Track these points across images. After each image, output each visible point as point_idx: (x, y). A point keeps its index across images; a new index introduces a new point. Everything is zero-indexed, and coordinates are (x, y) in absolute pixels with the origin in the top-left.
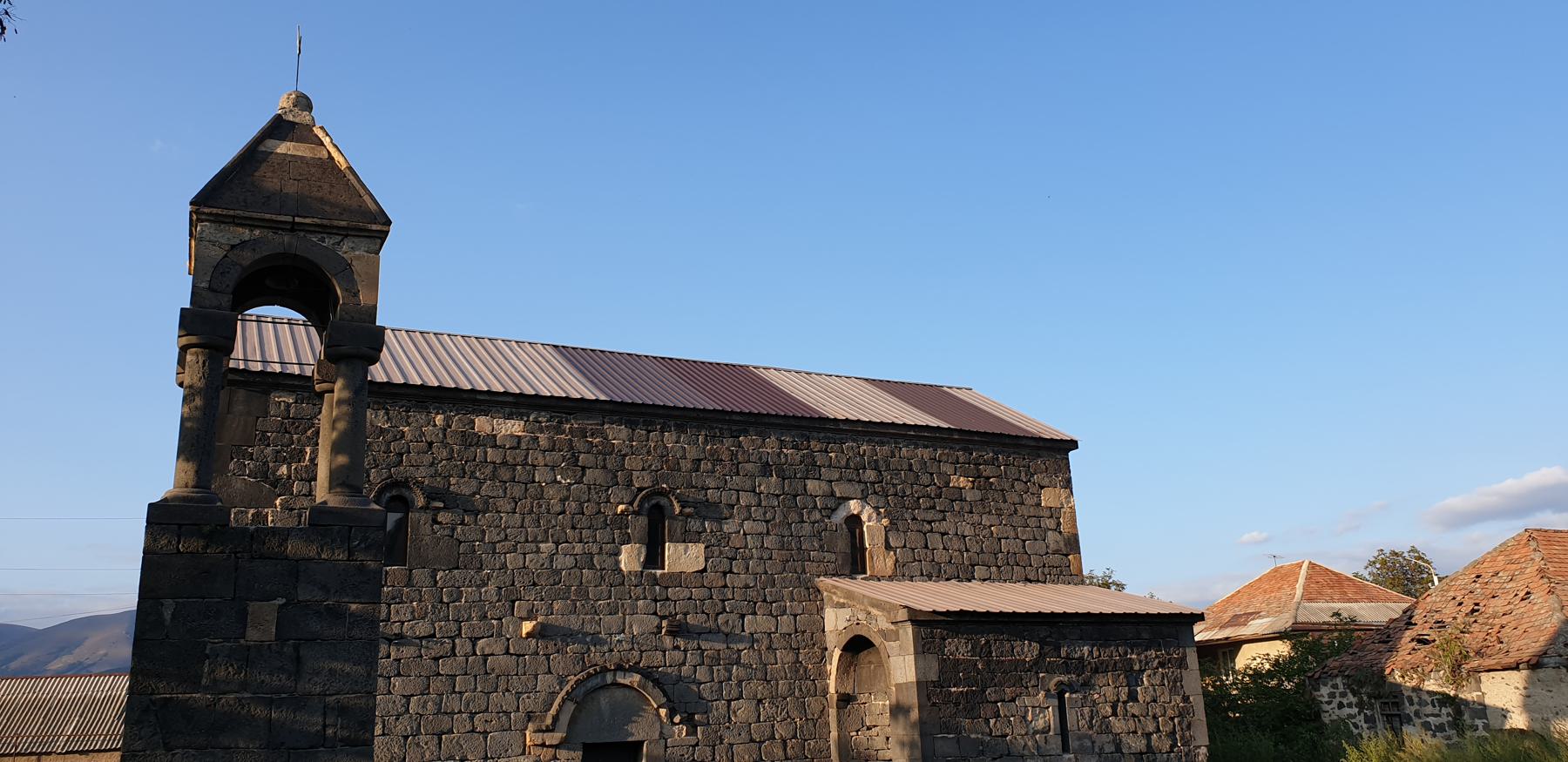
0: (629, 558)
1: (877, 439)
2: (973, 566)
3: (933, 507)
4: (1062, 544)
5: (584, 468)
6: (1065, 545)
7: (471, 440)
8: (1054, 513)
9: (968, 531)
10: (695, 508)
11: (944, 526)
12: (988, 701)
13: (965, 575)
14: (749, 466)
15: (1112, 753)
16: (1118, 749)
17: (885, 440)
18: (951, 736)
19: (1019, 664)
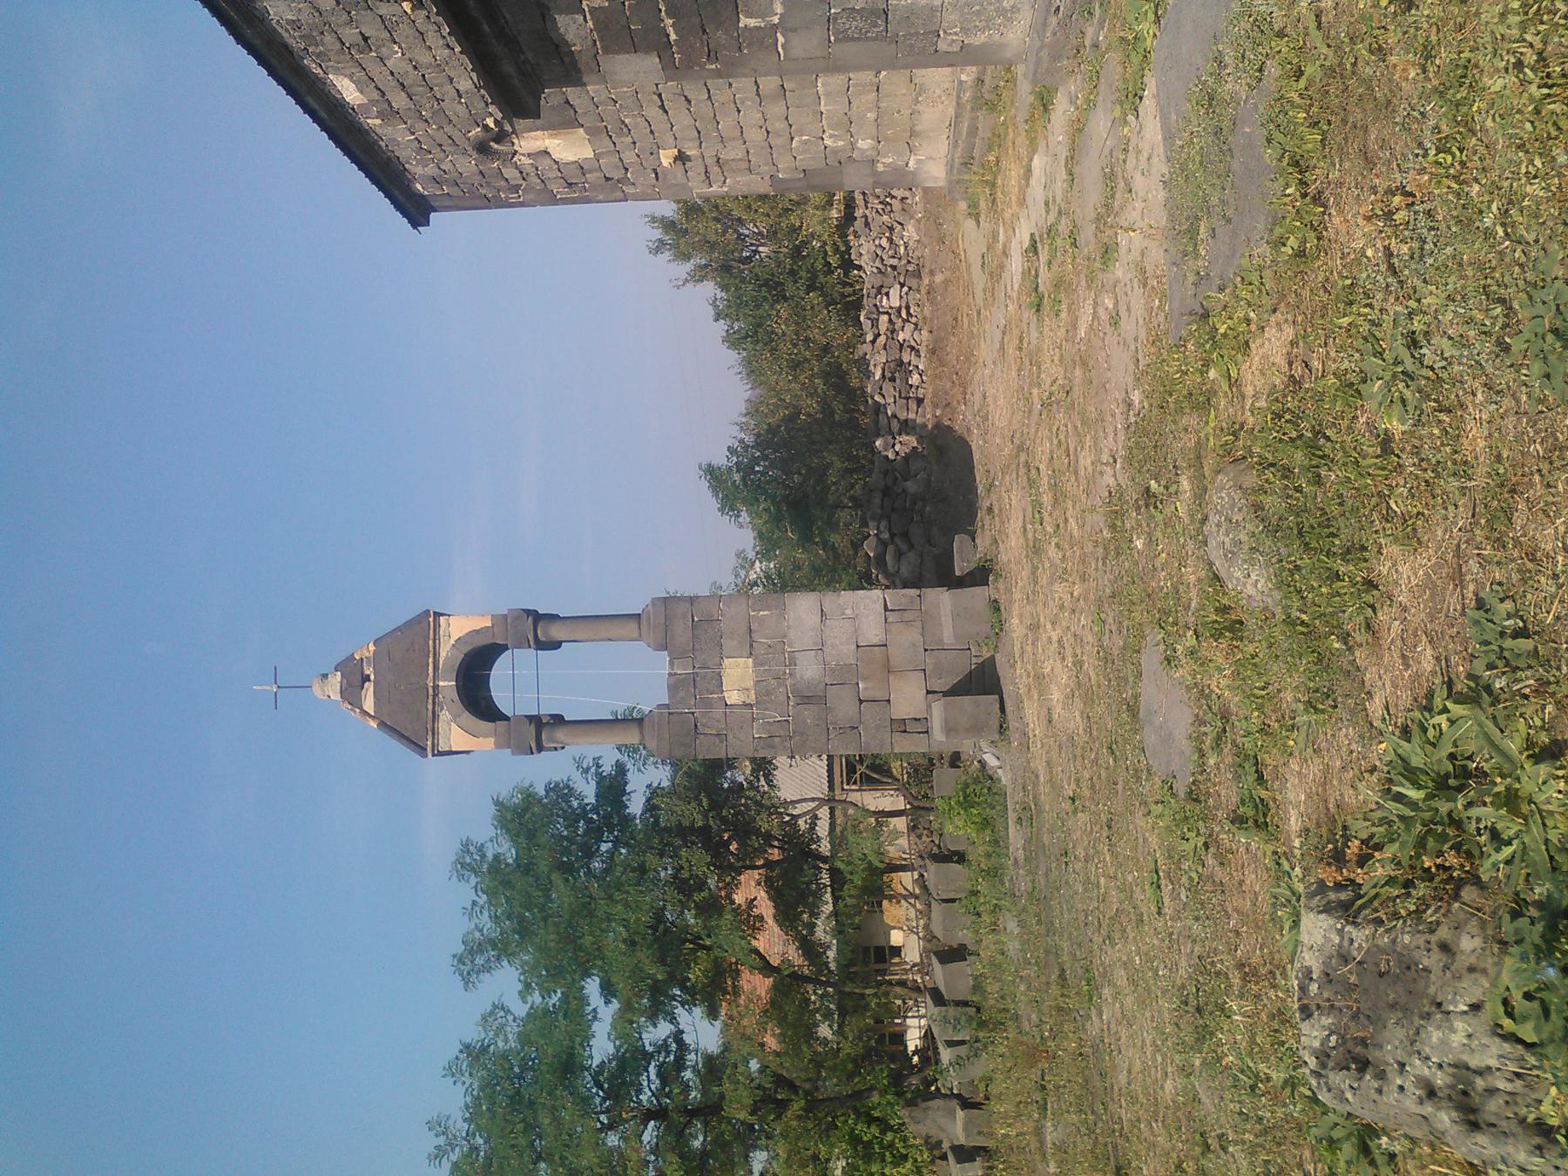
5: (365, 39)
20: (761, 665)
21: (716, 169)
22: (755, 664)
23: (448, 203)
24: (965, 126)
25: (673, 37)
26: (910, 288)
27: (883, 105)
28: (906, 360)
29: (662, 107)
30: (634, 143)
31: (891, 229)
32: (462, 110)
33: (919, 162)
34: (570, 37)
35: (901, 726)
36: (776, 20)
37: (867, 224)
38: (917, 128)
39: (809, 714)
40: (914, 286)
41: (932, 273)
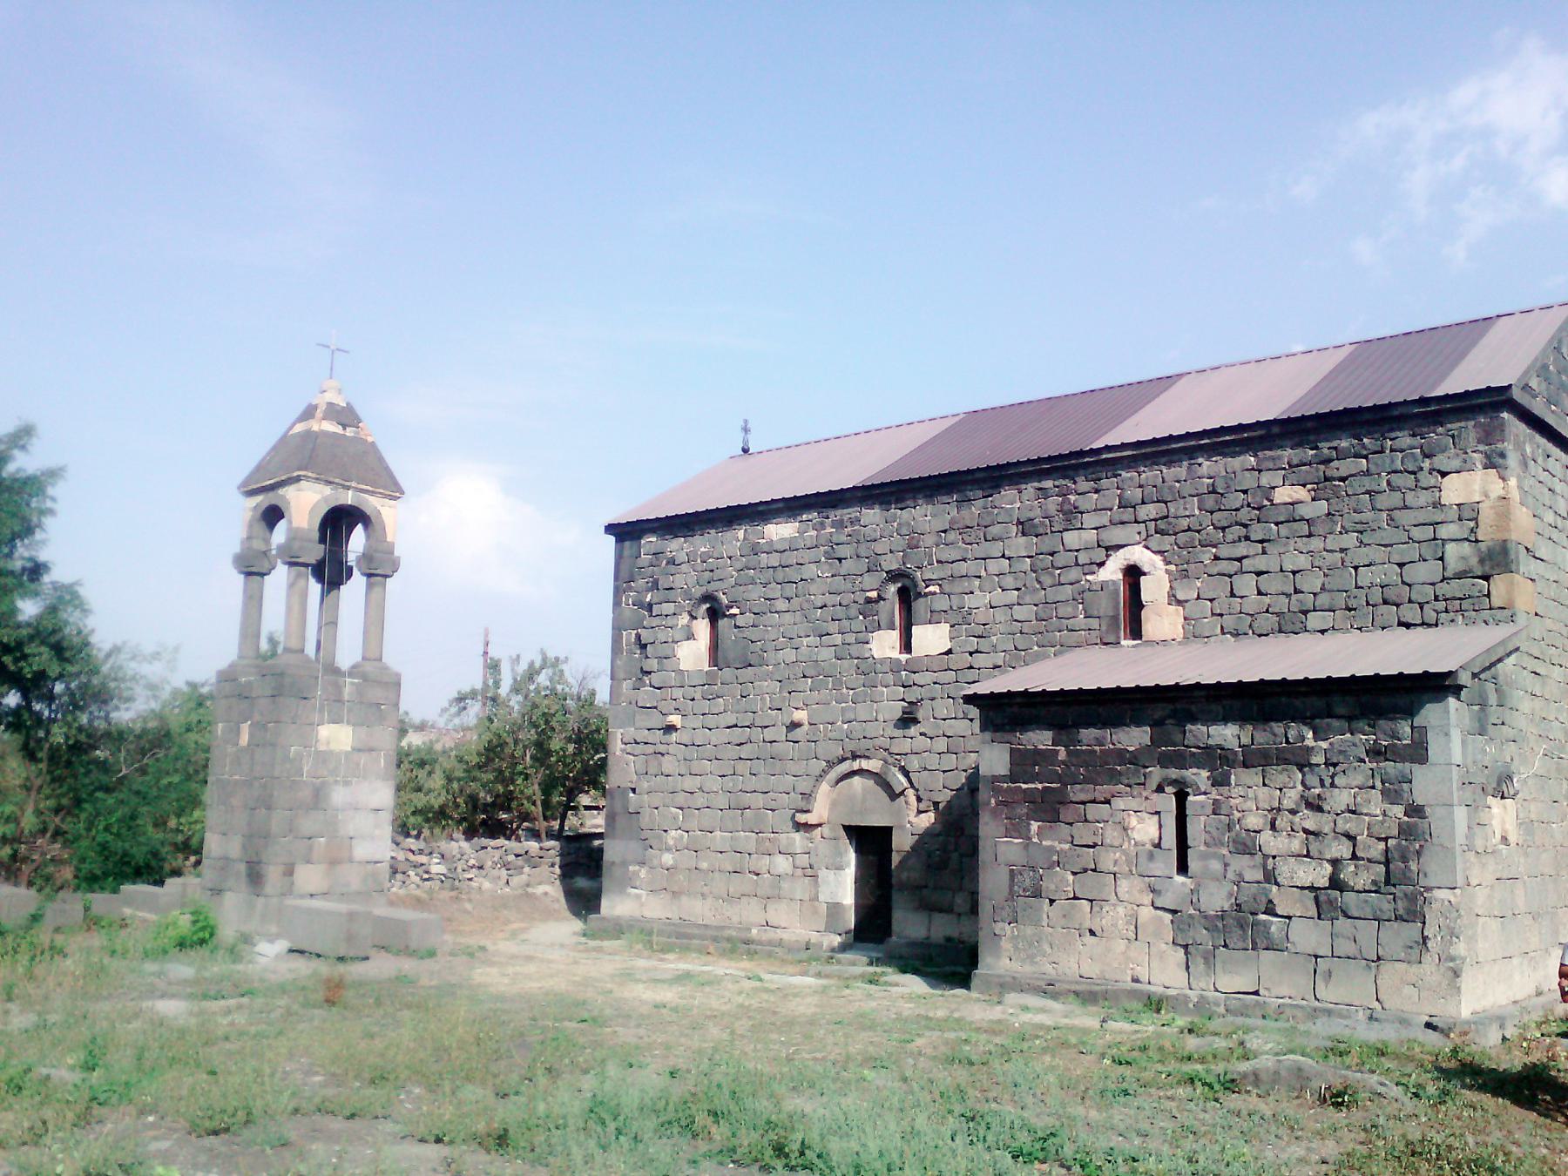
0: (885, 644)
1: (1164, 460)
2: (1305, 613)
3: (1247, 538)
4: (1474, 561)
5: (840, 560)
6: (1482, 561)
7: (755, 550)
8: (1468, 513)
9: (1303, 562)
10: (940, 585)
11: (1260, 563)
12: (1072, 802)
13: (1290, 624)
14: (995, 530)
15: (1259, 882)
16: (1270, 877)
17: (1175, 458)
18: (1016, 841)
19: (1121, 756)
20: (346, 758)
21: (651, 751)
22: (347, 753)
23: (626, 553)
24: (696, 931)
25: (1024, 786)
26: (442, 882)
27: (717, 874)
28: (399, 876)
29: (736, 726)
30: (693, 700)
31: (481, 868)
32: (754, 596)
33: (638, 897)
34: (1030, 734)
35: (289, 872)
36: (1035, 840)
37: (484, 848)
38: (684, 899)
39: (305, 794)
40: (445, 884)
41: (470, 900)
